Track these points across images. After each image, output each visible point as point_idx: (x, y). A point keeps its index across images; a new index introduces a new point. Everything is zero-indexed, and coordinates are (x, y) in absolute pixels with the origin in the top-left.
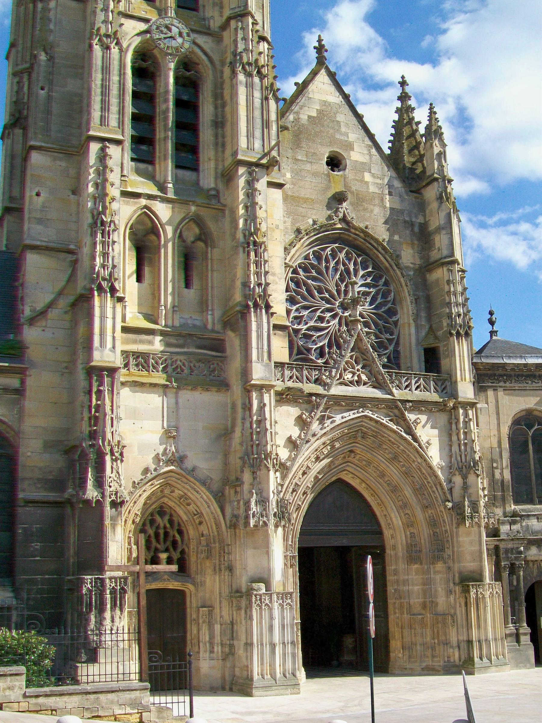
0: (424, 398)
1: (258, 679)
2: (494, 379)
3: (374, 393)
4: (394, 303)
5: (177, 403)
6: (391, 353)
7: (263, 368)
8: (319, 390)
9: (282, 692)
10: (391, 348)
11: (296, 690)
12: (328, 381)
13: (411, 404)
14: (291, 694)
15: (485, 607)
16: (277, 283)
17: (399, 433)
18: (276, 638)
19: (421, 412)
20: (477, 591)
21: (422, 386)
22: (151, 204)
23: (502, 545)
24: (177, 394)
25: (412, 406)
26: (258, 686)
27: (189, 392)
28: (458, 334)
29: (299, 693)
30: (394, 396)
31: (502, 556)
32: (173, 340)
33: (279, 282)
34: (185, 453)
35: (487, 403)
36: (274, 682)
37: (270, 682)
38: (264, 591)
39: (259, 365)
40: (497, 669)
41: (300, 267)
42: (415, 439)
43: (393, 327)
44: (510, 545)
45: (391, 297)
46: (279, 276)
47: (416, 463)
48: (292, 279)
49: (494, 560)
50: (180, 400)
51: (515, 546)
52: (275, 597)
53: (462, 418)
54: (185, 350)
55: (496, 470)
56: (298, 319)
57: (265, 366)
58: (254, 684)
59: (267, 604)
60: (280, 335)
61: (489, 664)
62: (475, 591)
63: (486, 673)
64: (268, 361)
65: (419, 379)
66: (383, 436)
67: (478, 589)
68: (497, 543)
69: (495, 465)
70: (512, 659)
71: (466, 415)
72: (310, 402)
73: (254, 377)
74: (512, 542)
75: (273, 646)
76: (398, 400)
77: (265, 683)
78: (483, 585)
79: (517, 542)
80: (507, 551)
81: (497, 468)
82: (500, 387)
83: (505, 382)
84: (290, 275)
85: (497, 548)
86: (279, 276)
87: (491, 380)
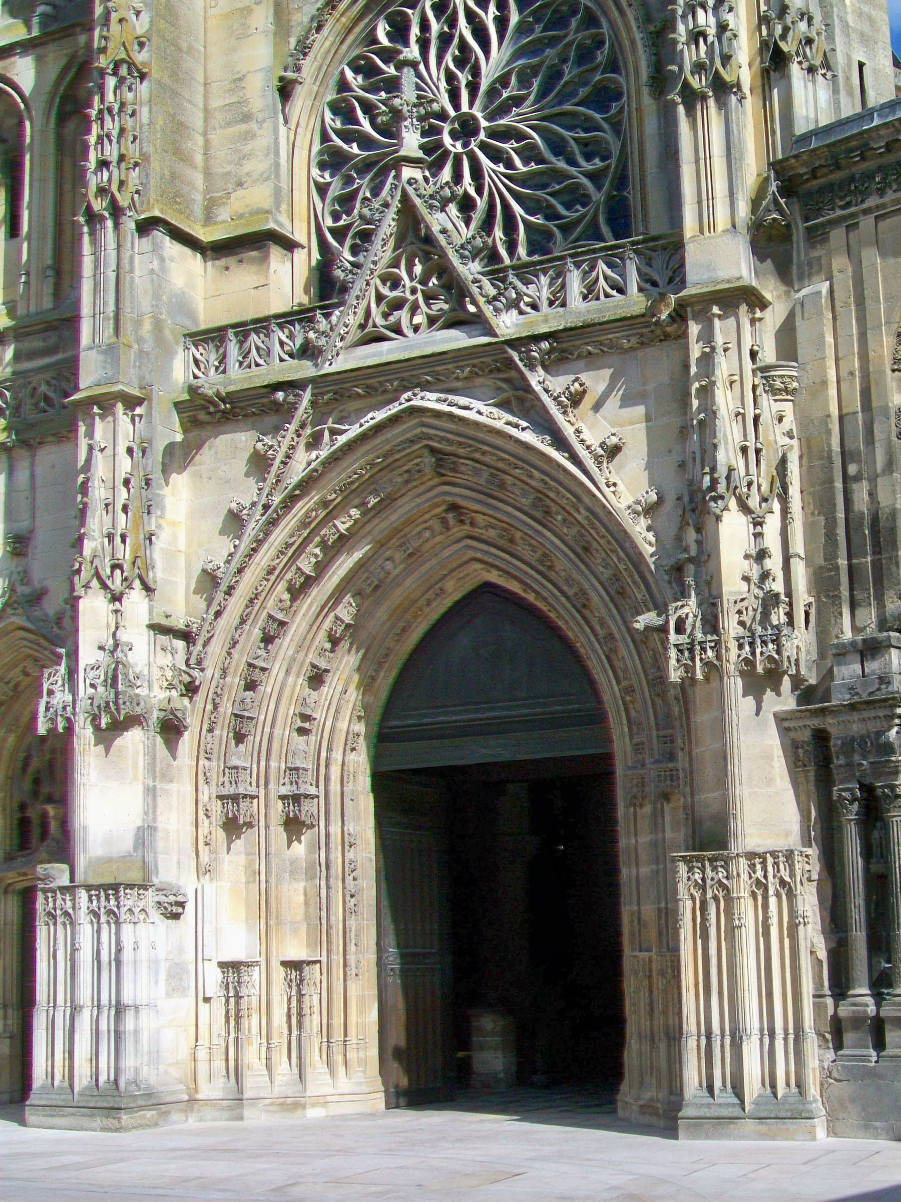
0: (595, 317)
1: (43, 1087)
2: (850, 192)
3: (450, 340)
4: (613, 66)
5: (33, 476)
6: (597, 210)
7: (101, 358)
8: (305, 369)
9: (85, 1122)
10: (598, 196)
11: (113, 1123)
12: (322, 341)
13: (545, 345)
14: (104, 1129)
15: (732, 930)
16: (254, 136)
17: (511, 437)
18: (85, 994)
19: (592, 361)
20: (703, 879)
21: (602, 281)
22: (6, 68)
23: (830, 724)
24: (33, 456)
25: (549, 353)
26: (37, 1103)
27: (54, 448)
28: (691, 98)
29: (117, 1130)
30: (496, 335)
31: (839, 761)
32: (36, 343)
33: (259, 132)
34: (45, 583)
35: (830, 278)
36: (71, 1097)
37: (63, 1097)
38: (65, 881)
39: (93, 354)
40: (763, 1128)
41: (357, 70)
42: (560, 442)
43: (608, 135)
44: (855, 726)
45: (601, 57)
46: (260, 116)
47: (583, 511)
48: (335, 108)
49: (812, 778)
50: (39, 470)
51: (873, 727)
52: (83, 895)
53: (696, 351)
54: (60, 356)
55: (855, 486)
56: (347, 201)
57: (105, 353)
58: (32, 1096)
59: (66, 914)
60: (253, 261)
61: (737, 1111)
62: (698, 877)
63: (720, 1137)
64: (114, 339)
65: (593, 268)
66: (484, 453)
67: (709, 873)
68: (815, 722)
69: (852, 469)
70: (853, 1101)
71: (707, 336)
72: (277, 407)
73: (82, 386)
74: (855, 716)
75: (75, 1009)
76: (513, 343)
77: (54, 1096)
78: (726, 861)
79: (872, 714)
80: (849, 745)
81: (858, 478)
82: (866, 212)
83: (881, 192)
84: (331, 96)
85: (821, 737)
86: (260, 116)
87: (841, 199)
